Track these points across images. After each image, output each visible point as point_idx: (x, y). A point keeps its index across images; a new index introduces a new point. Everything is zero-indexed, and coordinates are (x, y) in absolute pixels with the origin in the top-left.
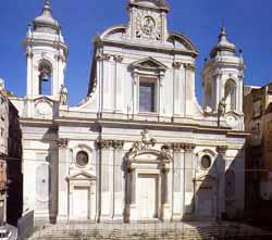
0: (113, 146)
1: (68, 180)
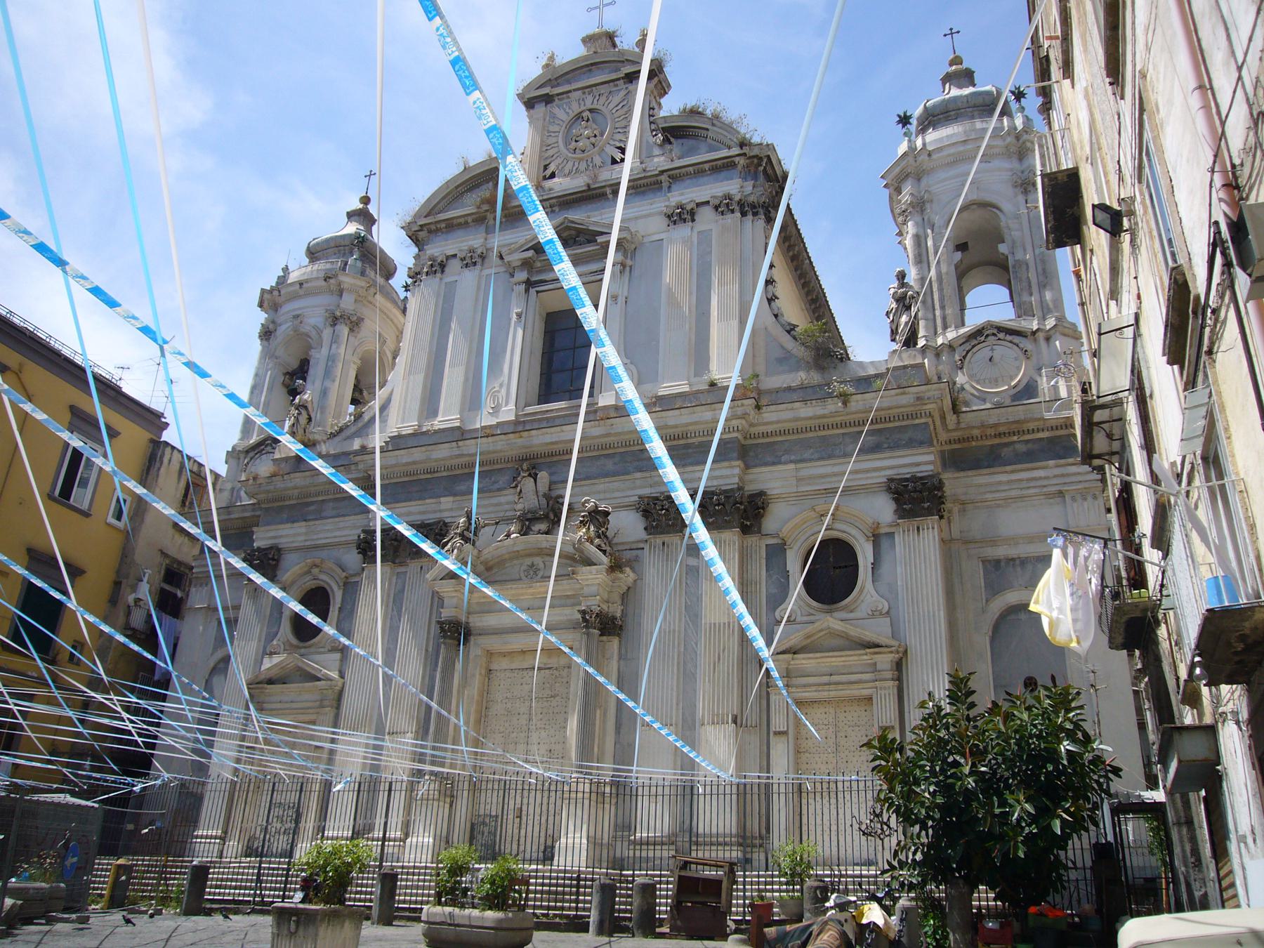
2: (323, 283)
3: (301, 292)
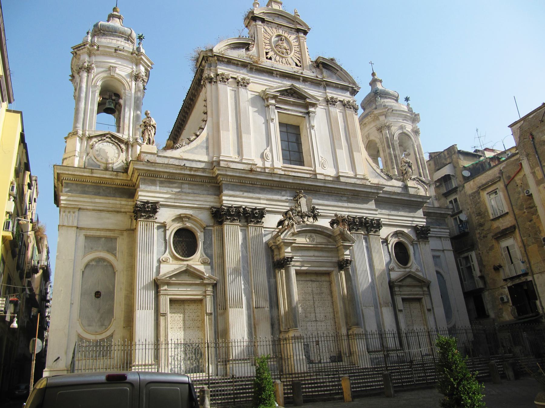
1: (157, 285)
2: (130, 55)
3: (114, 54)
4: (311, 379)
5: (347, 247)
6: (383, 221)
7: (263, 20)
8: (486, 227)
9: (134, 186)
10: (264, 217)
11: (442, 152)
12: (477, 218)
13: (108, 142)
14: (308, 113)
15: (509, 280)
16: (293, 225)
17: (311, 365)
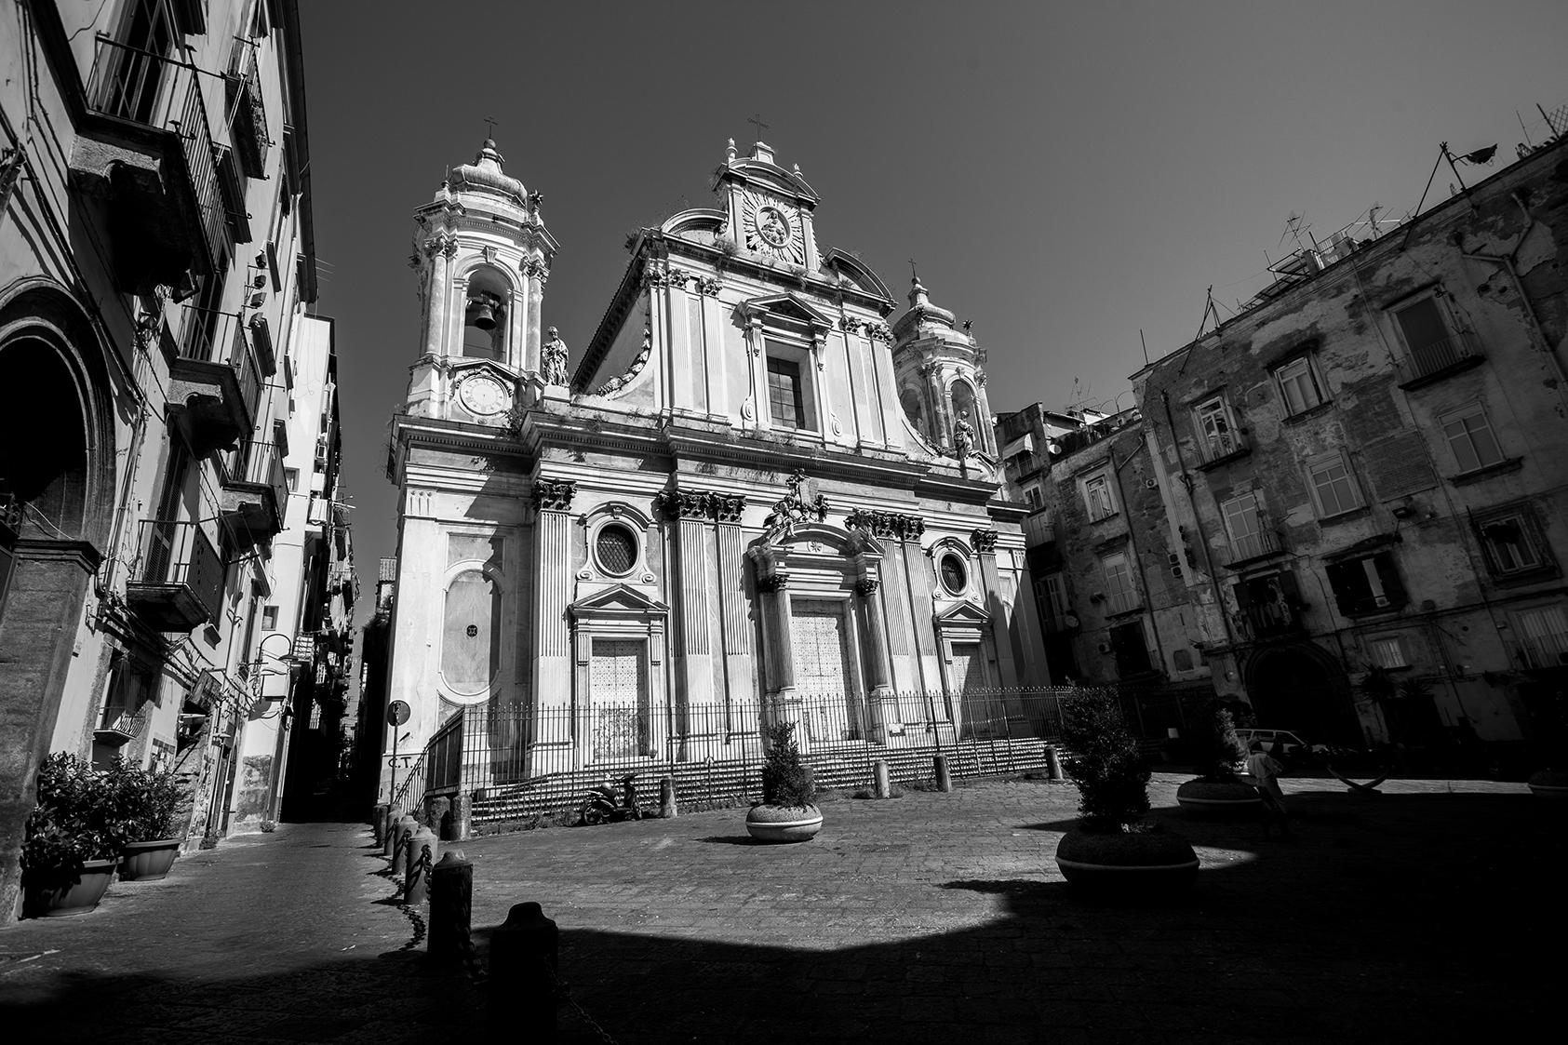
0: (713, 514)
1: (572, 616)
4: (826, 765)
5: (871, 563)
6: (926, 521)
7: (743, 182)
8: (1082, 536)
9: (530, 454)
10: (743, 510)
11: (1018, 414)
12: (1068, 520)
13: (485, 377)
14: (813, 343)
15: (1114, 619)
16: (789, 524)
17: (813, 745)
